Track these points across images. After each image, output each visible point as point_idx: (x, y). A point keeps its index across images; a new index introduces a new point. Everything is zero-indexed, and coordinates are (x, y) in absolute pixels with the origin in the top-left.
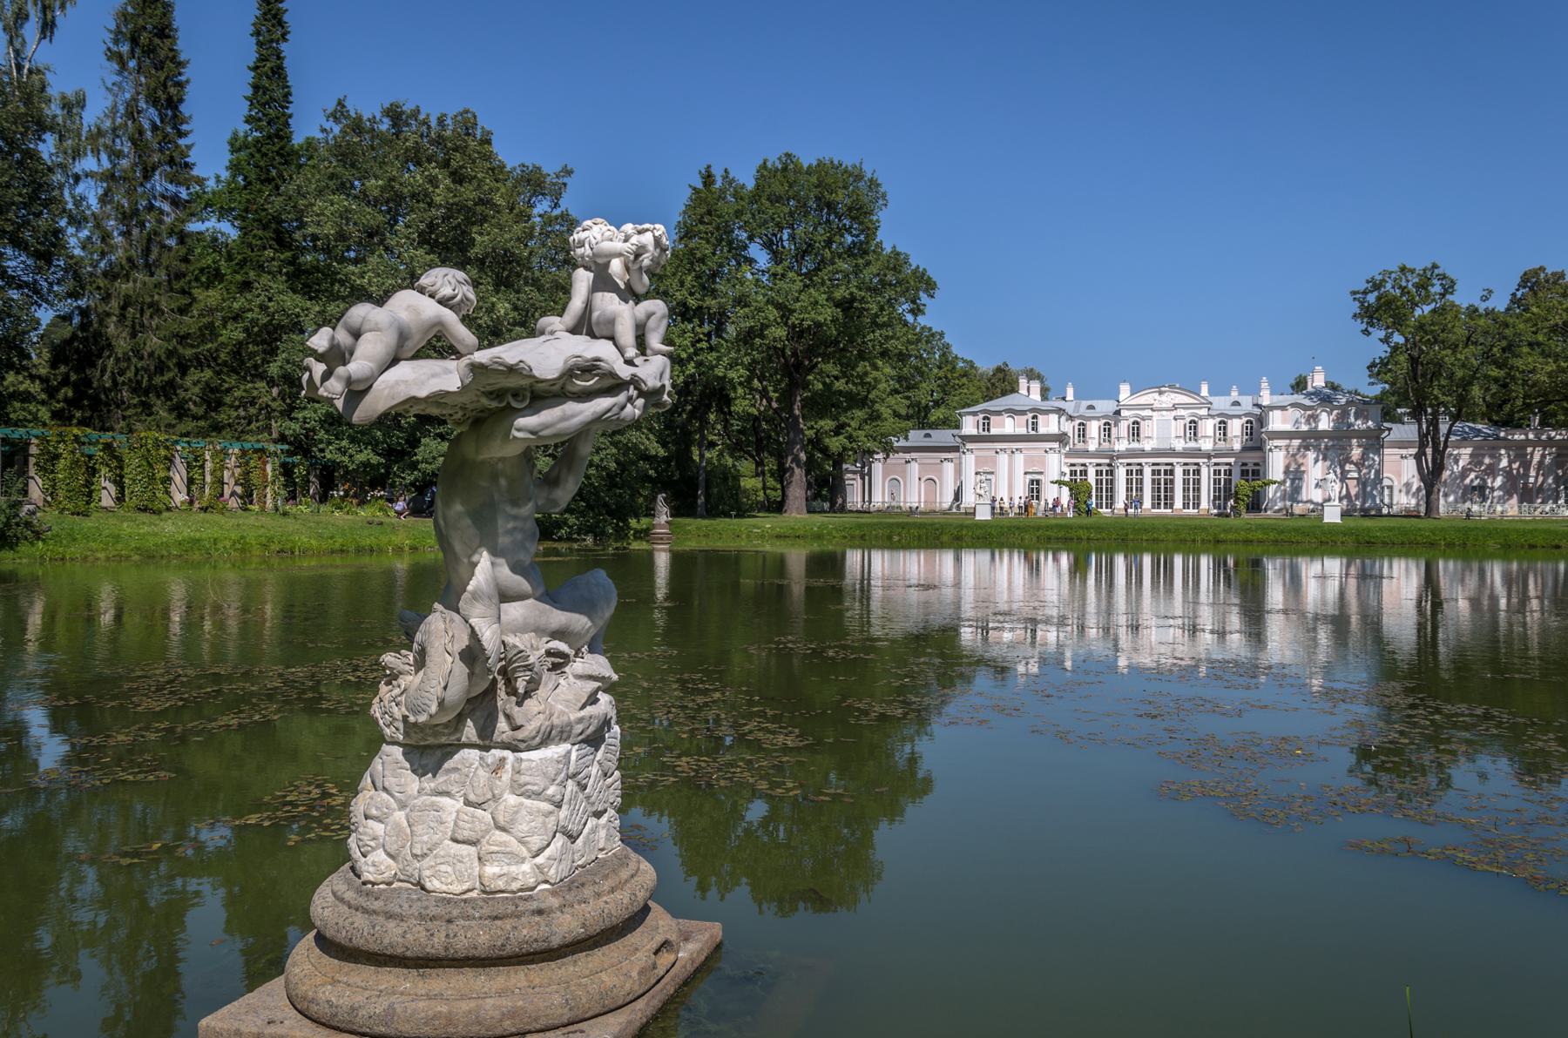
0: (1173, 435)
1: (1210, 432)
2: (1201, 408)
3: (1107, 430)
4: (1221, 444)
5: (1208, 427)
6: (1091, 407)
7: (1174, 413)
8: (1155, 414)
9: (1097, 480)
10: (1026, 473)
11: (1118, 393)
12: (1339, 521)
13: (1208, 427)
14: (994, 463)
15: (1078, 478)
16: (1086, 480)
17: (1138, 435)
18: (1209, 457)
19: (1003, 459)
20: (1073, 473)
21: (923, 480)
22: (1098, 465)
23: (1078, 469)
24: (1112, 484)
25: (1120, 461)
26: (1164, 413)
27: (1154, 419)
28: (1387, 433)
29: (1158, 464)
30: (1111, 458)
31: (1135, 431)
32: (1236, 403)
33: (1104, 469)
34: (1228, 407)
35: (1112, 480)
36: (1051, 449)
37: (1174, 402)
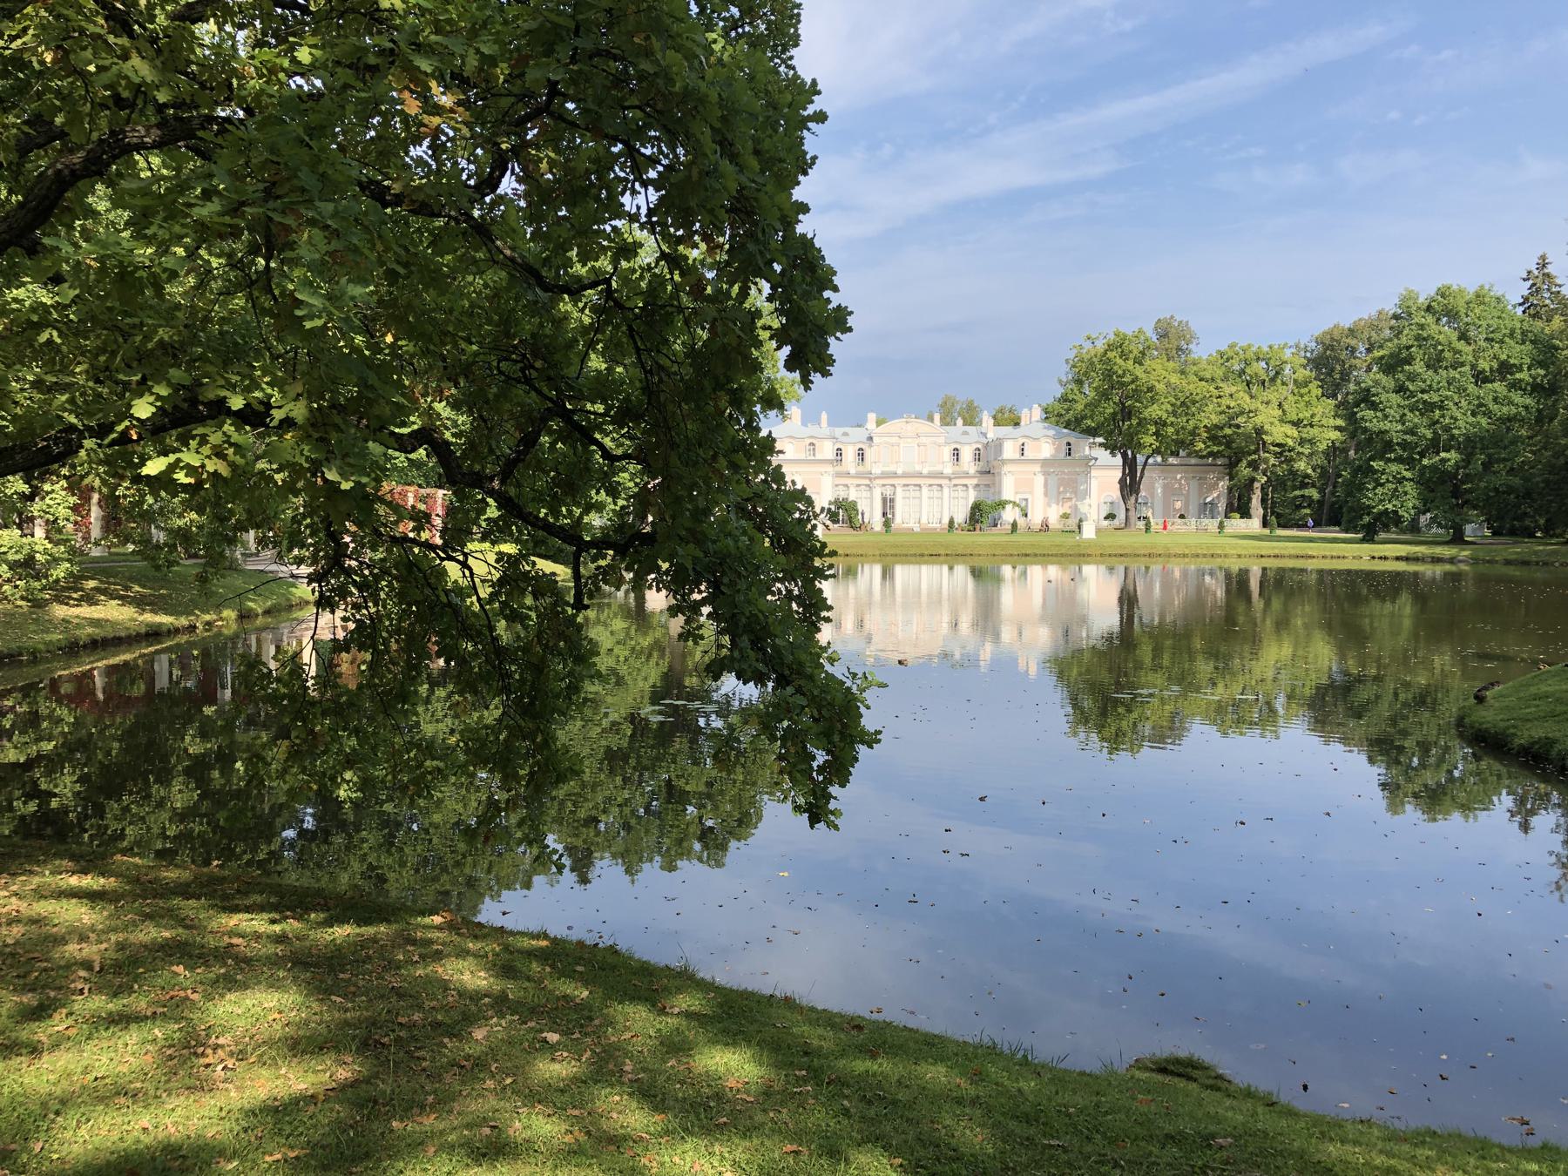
3: (861, 455)
4: (957, 468)
6: (845, 434)
8: (901, 441)
11: (865, 420)
18: (950, 479)
30: (870, 479)
32: (965, 433)
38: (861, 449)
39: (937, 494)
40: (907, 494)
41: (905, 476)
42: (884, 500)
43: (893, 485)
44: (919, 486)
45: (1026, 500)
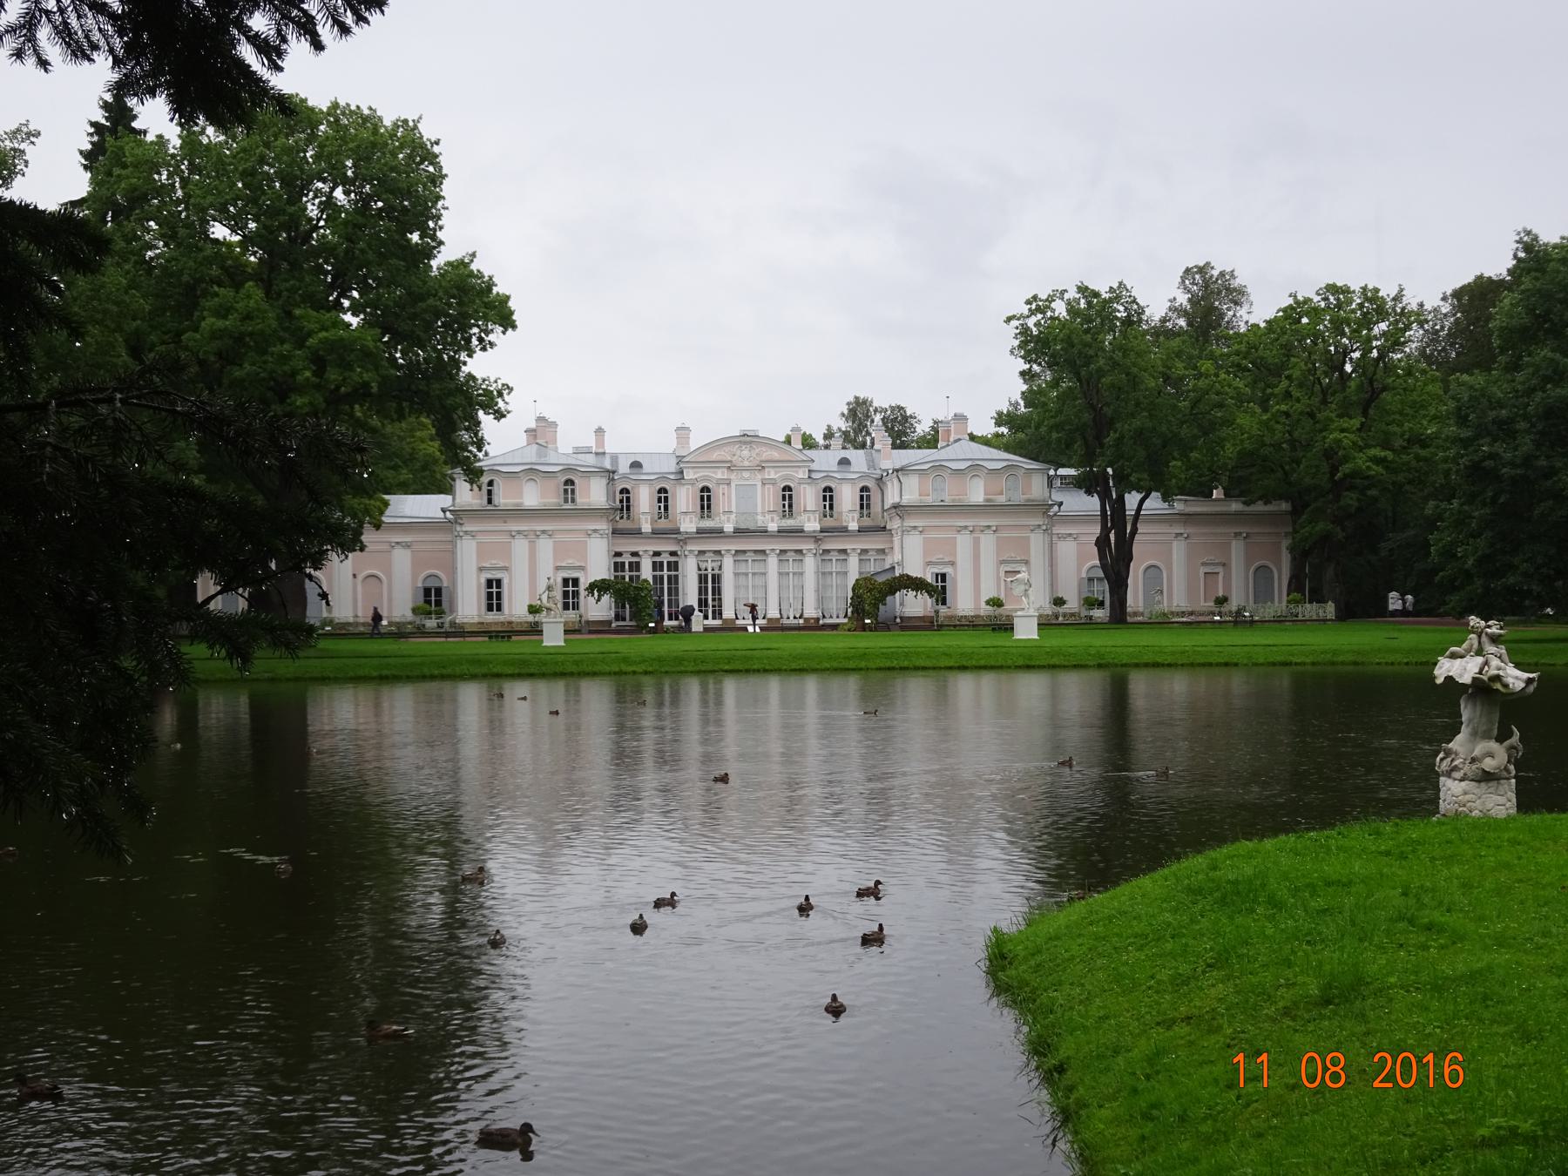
0: (759, 510)
1: (811, 505)
2: (799, 467)
3: (663, 496)
4: (829, 522)
5: (808, 498)
7: (759, 476)
8: (733, 476)
9: (655, 577)
10: (558, 568)
12: (1036, 637)
13: (808, 498)
14: (507, 552)
15: (627, 575)
16: (638, 577)
17: (709, 507)
18: (817, 540)
19: (520, 547)
20: (618, 567)
21: (360, 577)
22: (657, 554)
23: (627, 559)
24: (677, 582)
25: (689, 548)
26: (746, 474)
27: (733, 485)
28: (1056, 508)
29: (744, 552)
31: (706, 500)
33: (665, 559)
34: (835, 468)
35: (676, 576)
36: (595, 531)
37: (763, 458)
38: (663, 490)
39: (791, 567)
40: (742, 568)
41: (739, 532)
42: (702, 579)
43: (718, 553)
44: (763, 552)
45: (944, 576)
